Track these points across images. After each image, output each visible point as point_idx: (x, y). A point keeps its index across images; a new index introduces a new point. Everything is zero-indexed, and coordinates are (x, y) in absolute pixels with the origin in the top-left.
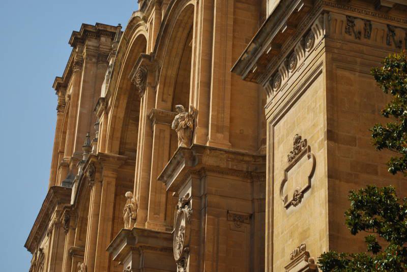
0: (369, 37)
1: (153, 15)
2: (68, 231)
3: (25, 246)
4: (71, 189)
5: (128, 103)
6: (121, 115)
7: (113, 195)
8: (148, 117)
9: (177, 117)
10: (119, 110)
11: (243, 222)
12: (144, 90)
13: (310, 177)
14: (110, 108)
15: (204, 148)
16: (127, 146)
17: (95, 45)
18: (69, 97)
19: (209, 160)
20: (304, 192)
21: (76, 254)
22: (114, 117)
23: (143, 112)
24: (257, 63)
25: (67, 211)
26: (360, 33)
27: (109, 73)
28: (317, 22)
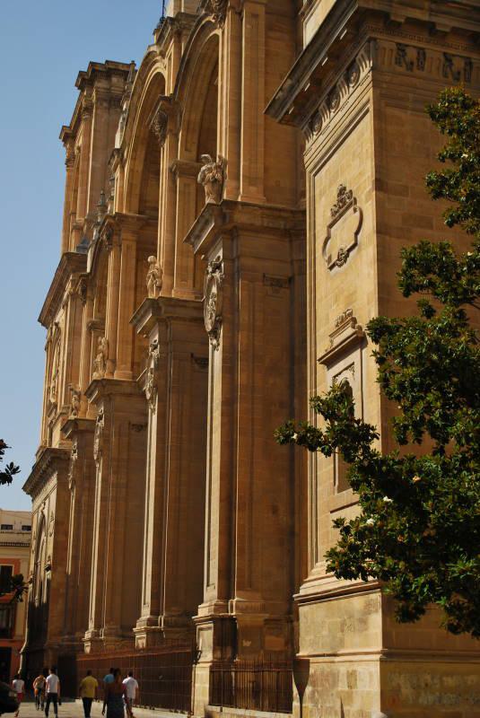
0: (423, 68)
1: (171, 50)
2: (85, 302)
3: (39, 321)
4: (86, 256)
5: (146, 154)
6: (140, 167)
7: (134, 261)
8: (170, 169)
9: (203, 168)
10: (137, 162)
11: (281, 286)
12: (164, 138)
13: (357, 233)
14: (126, 160)
15: (236, 203)
16: (148, 204)
17: (105, 86)
18: (79, 148)
19: (240, 218)
20: (349, 250)
21: (96, 328)
22: (131, 171)
23: (164, 165)
24: (294, 102)
25: (83, 280)
26: (412, 63)
27: (124, 119)
28: (362, 52)
